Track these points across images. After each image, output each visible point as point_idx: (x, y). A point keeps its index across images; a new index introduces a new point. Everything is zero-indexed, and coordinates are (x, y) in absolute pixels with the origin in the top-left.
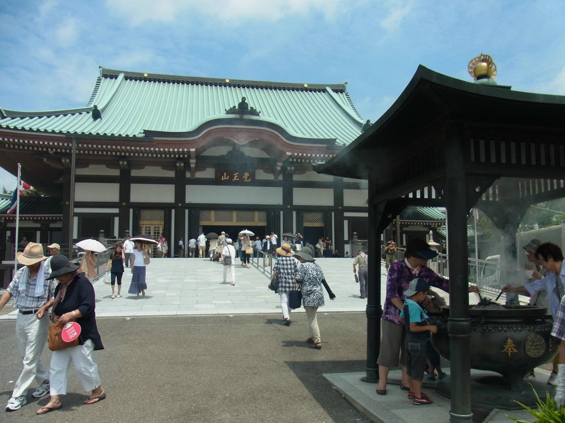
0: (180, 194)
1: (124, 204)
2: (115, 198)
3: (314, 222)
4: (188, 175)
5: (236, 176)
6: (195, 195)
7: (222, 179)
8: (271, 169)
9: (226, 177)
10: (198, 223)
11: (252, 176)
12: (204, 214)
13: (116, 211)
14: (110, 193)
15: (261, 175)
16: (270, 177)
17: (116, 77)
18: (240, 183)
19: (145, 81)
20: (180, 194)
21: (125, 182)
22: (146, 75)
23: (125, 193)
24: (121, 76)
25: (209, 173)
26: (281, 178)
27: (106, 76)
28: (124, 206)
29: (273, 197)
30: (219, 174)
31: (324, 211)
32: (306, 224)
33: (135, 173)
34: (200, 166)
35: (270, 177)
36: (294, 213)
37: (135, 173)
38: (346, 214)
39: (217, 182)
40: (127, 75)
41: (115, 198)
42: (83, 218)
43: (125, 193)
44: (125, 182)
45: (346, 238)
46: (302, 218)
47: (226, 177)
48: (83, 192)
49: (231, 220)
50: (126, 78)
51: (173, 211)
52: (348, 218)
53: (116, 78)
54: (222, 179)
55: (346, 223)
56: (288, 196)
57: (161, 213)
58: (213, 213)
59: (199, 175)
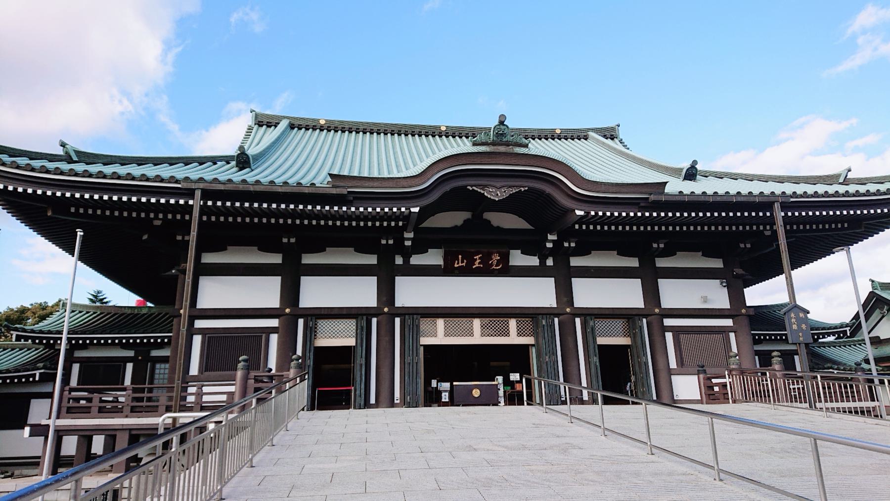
0: (387, 292)
1: (288, 310)
2: (273, 300)
3: (613, 337)
4: (399, 260)
5: (478, 261)
6: (411, 292)
7: (456, 265)
9: (462, 262)
10: (418, 341)
11: (505, 258)
12: (425, 324)
13: (274, 323)
15: (518, 259)
16: (534, 261)
18: (486, 271)
19: (322, 130)
20: (387, 292)
22: (322, 122)
23: (291, 293)
25: (434, 258)
26: (550, 262)
27: (260, 124)
28: (287, 314)
29: (540, 293)
30: (449, 258)
31: (628, 316)
32: (601, 341)
33: (308, 259)
34: (420, 247)
35: (534, 261)
36: (578, 321)
38: (668, 322)
39: (447, 270)
40: (293, 122)
41: (273, 300)
43: (291, 293)
45: (673, 364)
46: (593, 329)
47: (462, 262)
48: (215, 293)
49: (472, 335)
50: (292, 127)
51: (374, 321)
52: (672, 329)
53: (276, 126)
54: (456, 265)
55: (669, 336)
56: (565, 292)
59: (416, 260)
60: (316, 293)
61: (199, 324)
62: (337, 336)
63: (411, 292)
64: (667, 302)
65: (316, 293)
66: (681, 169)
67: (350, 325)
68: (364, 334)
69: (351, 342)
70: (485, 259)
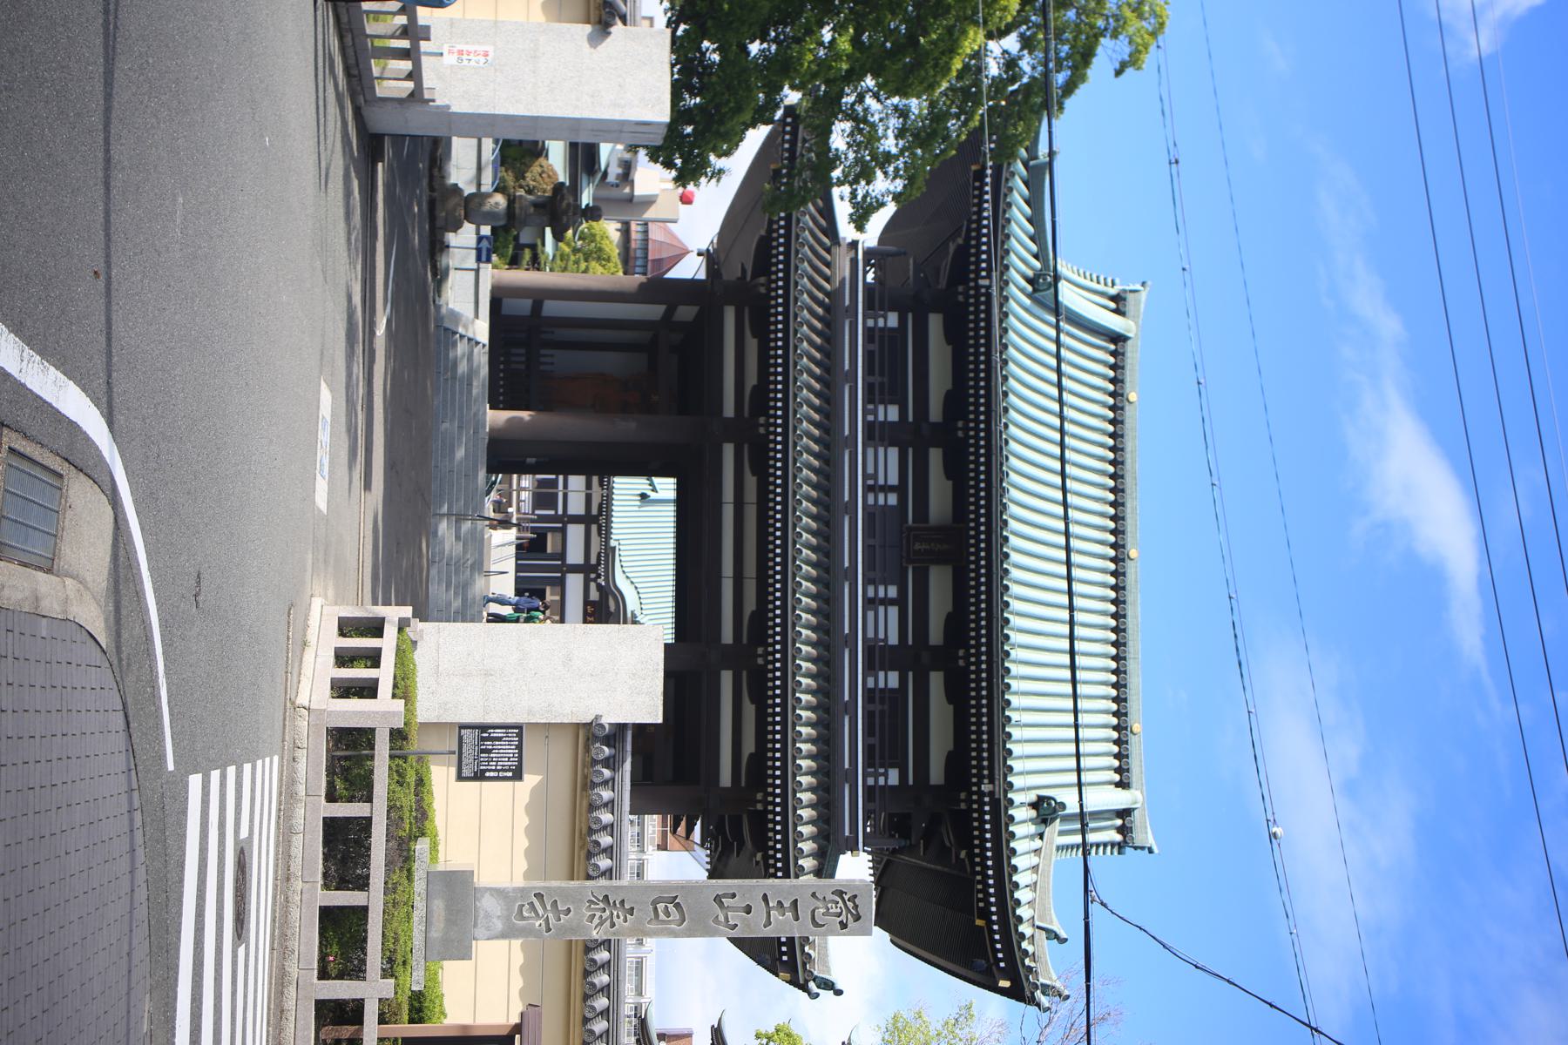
0: (575, 569)
6: (574, 582)
13: (560, 512)
14: (576, 506)
20: (575, 569)
21: (587, 519)
23: (576, 519)
25: (594, 595)
30: (593, 604)
33: (594, 528)
34: (599, 587)
37: (594, 528)
39: (587, 602)
42: (554, 484)
43: (576, 519)
44: (587, 519)
57: (559, 549)
59: (593, 585)
60: (575, 533)
61: (561, 478)
62: (551, 545)
63: (574, 582)
65: (575, 533)
66: (829, 972)
67: (559, 549)
68: (553, 557)
69: (549, 550)
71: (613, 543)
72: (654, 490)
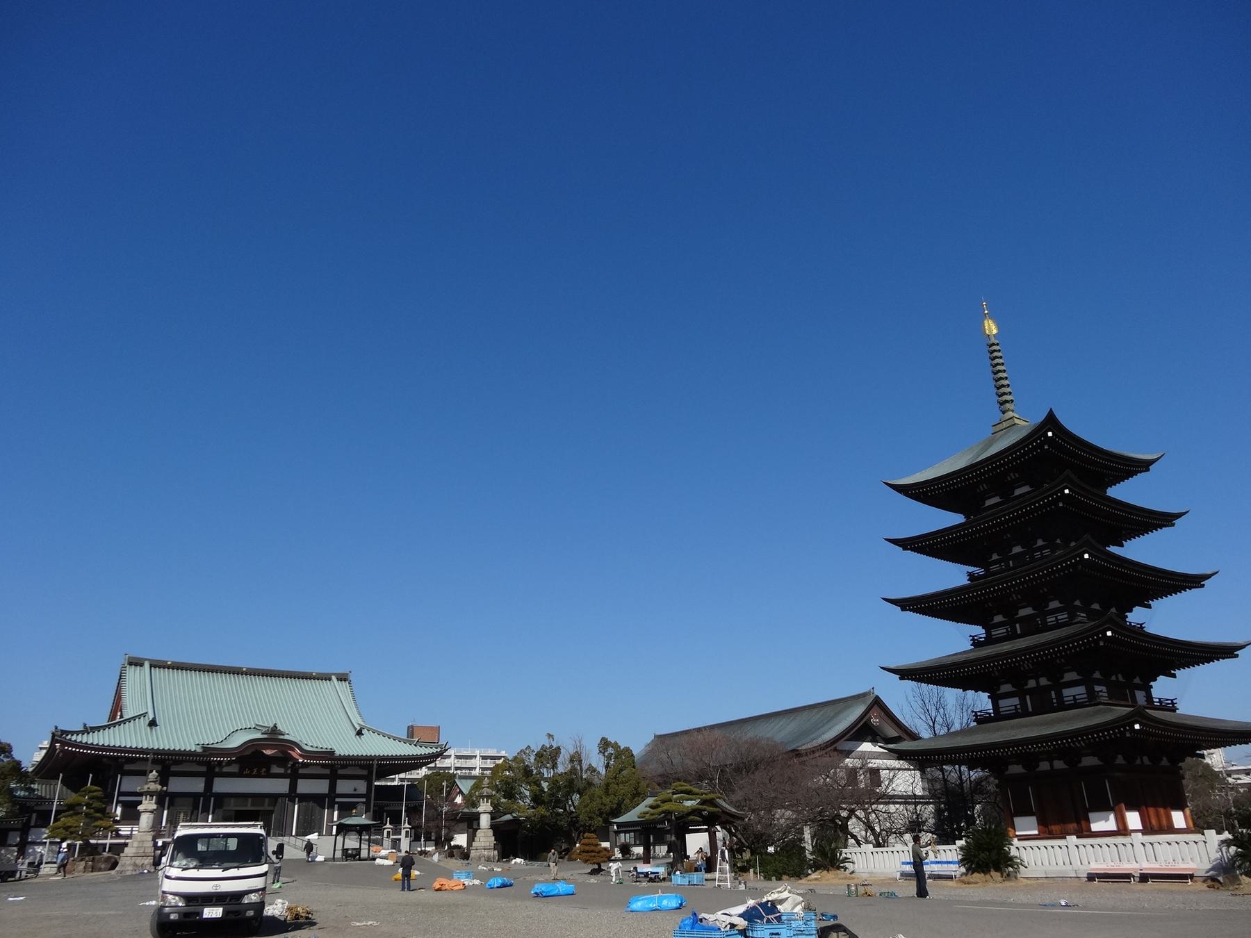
0: (209, 785)
4: (217, 770)
8: (285, 767)
11: (269, 769)
15: (275, 769)
16: (281, 771)
17: (142, 665)
18: (259, 776)
20: (209, 785)
24: (147, 664)
25: (234, 769)
27: (130, 664)
29: (281, 786)
33: (173, 768)
35: (281, 771)
39: (240, 775)
57: (191, 800)
58: (232, 800)
59: (225, 770)
64: (339, 790)
70: (259, 771)
71: (199, 750)
72: (144, 715)
